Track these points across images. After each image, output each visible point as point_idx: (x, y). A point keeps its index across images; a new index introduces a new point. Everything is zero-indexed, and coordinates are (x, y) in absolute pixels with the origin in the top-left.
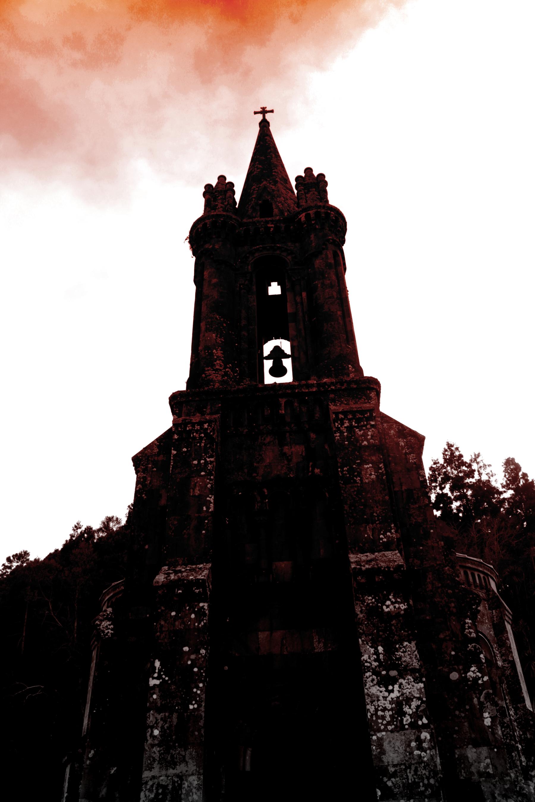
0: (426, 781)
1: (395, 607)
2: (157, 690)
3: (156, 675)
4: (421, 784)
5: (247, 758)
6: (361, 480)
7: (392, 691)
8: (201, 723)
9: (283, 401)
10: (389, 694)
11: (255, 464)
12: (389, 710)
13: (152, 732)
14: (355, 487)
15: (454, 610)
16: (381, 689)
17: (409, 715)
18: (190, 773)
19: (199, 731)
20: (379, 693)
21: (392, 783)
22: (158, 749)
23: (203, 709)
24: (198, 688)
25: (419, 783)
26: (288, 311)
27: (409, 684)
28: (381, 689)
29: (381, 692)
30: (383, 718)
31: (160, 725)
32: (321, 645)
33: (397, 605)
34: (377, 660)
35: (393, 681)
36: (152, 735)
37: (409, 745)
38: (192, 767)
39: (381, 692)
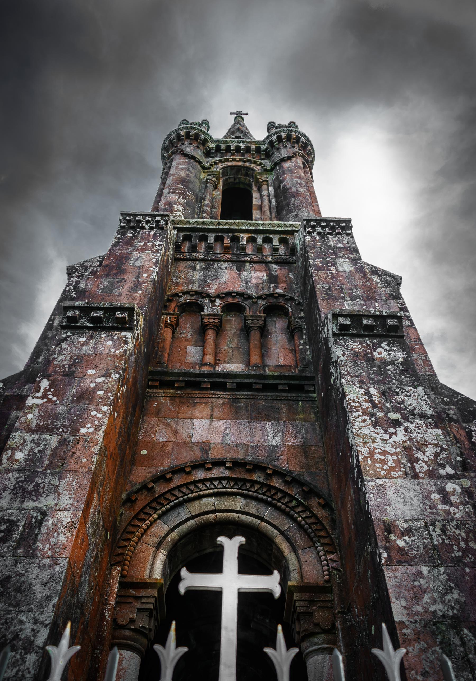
0: (463, 545)
1: (390, 354)
2: (36, 410)
3: (39, 394)
4: (455, 547)
5: (158, 562)
6: (337, 269)
7: (395, 434)
8: (96, 449)
9: (244, 237)
10: (390, 437)
11: (208, 281)
12: (392, 455)
13: (13, 454)
14: (330, 273)
15: (455, 417)
16: (378, 431)
17: (424, 462)
18: (62, 507)
19: (89, 457)
20: (374, 434)
21: (405, 542)
22: (17, 475)
23: (101, 433)
24: (99, 410)
25: (452, 546)
26: (253, 203)
27: (419, 429)
28: (376, 431)
29: (377, 433)
30: (383, 462)
31: (28, 448)
32: (278, 438)
33: (393, 354)
34: (371, 401)
35: (396, 423)
36: (11, 459)
37: (429, 497)
38: (67, 499)
39: (377, 433)
